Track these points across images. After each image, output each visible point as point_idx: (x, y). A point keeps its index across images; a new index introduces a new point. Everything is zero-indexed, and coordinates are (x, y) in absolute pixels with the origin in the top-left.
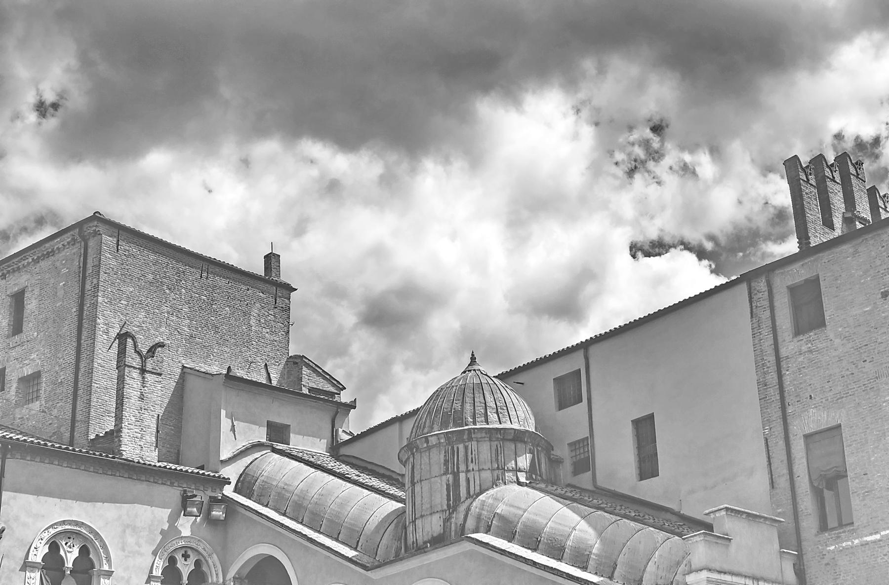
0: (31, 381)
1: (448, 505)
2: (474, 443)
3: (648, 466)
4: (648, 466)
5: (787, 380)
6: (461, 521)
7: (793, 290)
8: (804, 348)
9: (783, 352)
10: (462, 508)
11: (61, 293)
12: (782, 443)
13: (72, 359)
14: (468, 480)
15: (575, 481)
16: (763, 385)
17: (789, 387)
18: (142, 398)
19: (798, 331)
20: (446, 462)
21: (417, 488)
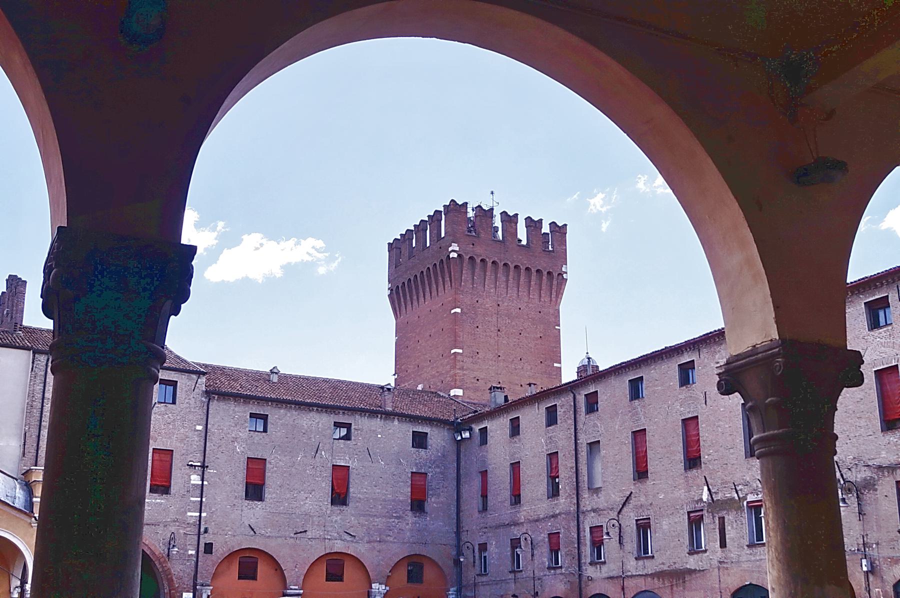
12: (34, 437)
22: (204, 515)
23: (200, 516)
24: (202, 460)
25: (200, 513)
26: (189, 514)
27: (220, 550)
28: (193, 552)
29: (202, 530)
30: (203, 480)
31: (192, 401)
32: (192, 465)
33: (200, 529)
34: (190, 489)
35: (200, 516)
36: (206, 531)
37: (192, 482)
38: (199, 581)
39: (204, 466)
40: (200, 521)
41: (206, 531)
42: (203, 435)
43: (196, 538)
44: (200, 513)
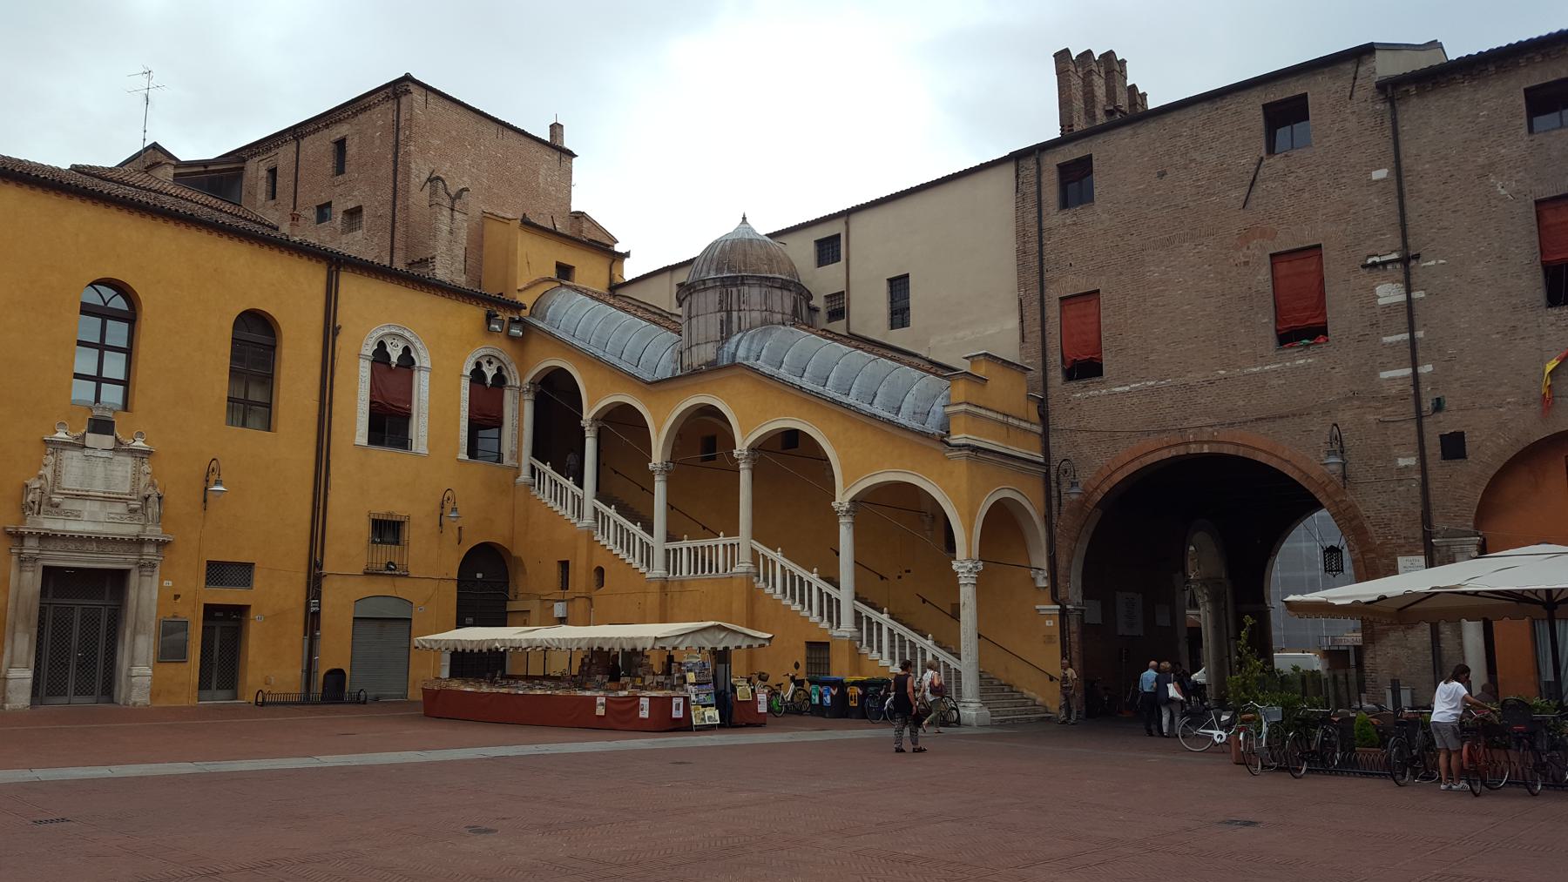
0: (354, 214)
3: (899, 315)
4: (899, 315)
5: (1047, 249)
6: (733, 349)
7: (1062, 168)
9: (1046, 224)
10: (735, 339)
11: (378, 142)
12: (1036, 304)
13: (390, 197)
15: (830, 327)
16: (1022, 253)
17: (1049, 256)
18: (451, 232)
19: (1065, 204)
20: (721, 302)
21: (694, 321)
23: (1415, 374)
24: (1398, 243)
25: (1415, 366)
26: (1385, 375)
27: (1490, 446)
28: (1412, 461)
29: (1427, 405)
32: (1374, 265)
33: (1420, 404)
34: (1380, 319)
35: (1415, 374)
36: (1438, 406)
37: (1381, 302)
38: (1439, 524)
39: (1405, 260)
41: (1438, 406)
42: (1394, 186)
43: (1413, 427)
44: (1415, 366)
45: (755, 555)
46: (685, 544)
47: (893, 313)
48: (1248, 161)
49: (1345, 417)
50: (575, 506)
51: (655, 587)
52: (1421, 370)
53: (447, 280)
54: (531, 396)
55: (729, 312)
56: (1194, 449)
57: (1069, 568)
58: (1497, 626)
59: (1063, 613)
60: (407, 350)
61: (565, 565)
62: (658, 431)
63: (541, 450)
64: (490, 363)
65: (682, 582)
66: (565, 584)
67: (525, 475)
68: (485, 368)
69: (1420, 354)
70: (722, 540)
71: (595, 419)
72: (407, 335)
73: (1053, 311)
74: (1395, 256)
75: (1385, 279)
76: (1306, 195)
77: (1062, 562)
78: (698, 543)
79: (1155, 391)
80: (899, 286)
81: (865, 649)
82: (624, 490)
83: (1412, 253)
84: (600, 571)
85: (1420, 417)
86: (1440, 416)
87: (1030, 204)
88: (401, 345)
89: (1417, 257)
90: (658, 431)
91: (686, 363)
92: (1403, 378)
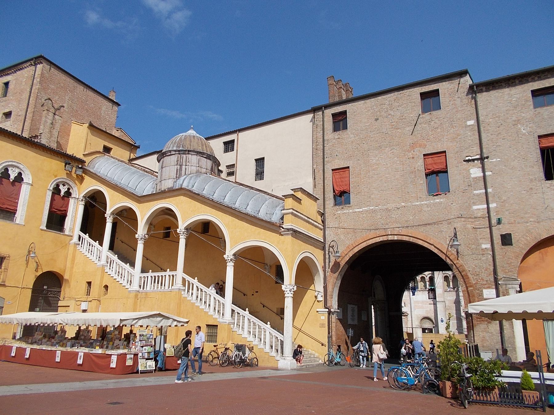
1: (176, 177)
2: (190, 155)
3: (260, 175)
4: (260, 175)
7: (334, 115)
8: (336, 137)
11: (24, 84)
12: (321, 171)
13: (26, 107)
14: (186, 169)
20: (177, 161)
21: (164, 169)
22: (492, 206)
23: (488, 208)
25: (488, 204)
26: (475, 207)
27: (523, 240)
28: (489, 246)
29: (494, 221)
30: (484, 171)
31: (458, 102)
32: (469, 161)
34: (471, 184)
35: (488, 208)
36: (499, 222)
37: (472, 176)
38: (500, 275)
40: (489, 212)
41: (499, 222)
44: (488, 204)
45: (184, 280)
46: (150, 274)
47: (257, 174)
48: (414, 116)
49: (458, 225)
50: (97, 255)
51: (132, 295)
52: (491, 206)
53: (47, 145)
54: (83, 203)
55: (181, 166)
56: (390, 238)
57: (333, 292)
58: (528, 322)
59: (330, 313)
60: (20, 174)
61: (89, 283)
62: (142, 219)
63: (84, 229)
64: (64, 185)
65: (146, 293)
66: (88, 293)
67: (75, 239)
68: (61, 187)
69: (490, 199)
70: (168, 273)
71: (112, 213)
72: (21, 166)
73: (329, 174)
74: (478, 157)
75: (474, 166)
76: (439, 130)
77: (330, 289)
78: (156, 274)
79: (374, 211)
80: (260, 162)
81: (235, 328)
82: (123, 250)
83: (485, 156)
84: (106, 287)
85: (490, 227)
86: (500, 226)
87: (320, 129)
88: (17, 171)
89: (487, 158)
90: (142, 219)
91: (158, 188)
92: (483, 209)
